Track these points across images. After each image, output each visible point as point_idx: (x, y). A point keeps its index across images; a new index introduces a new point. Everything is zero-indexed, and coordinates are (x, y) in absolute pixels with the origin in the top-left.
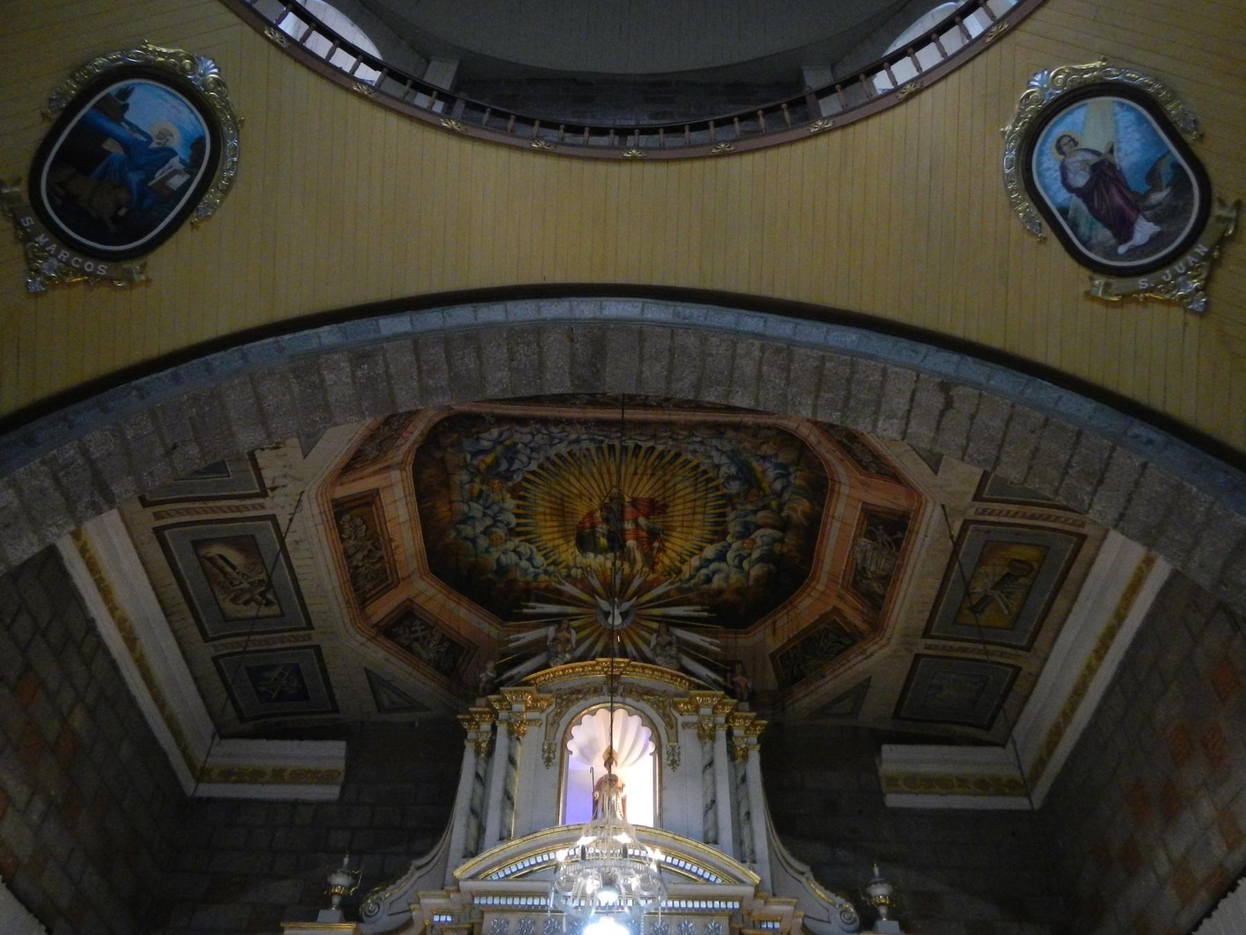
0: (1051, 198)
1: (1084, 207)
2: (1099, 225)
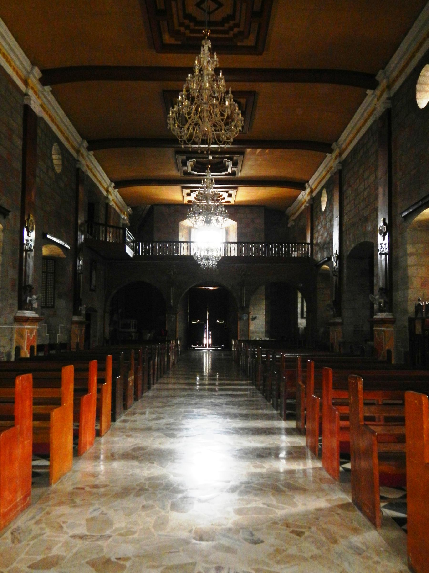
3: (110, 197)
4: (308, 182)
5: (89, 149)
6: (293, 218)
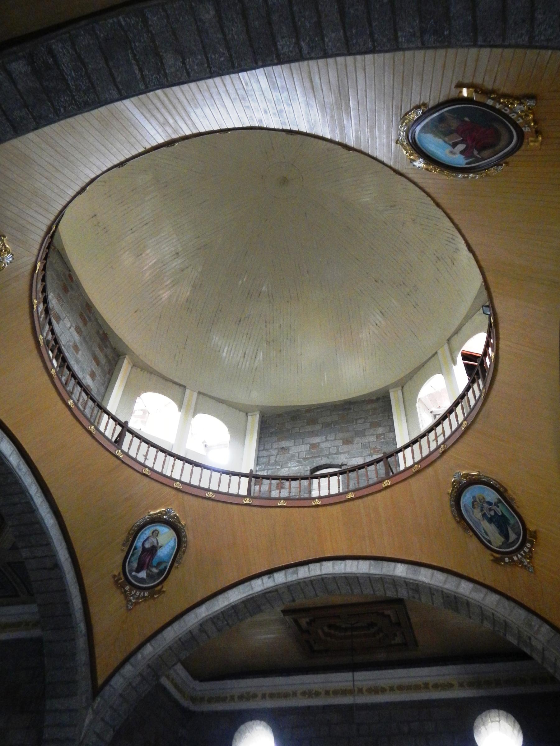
0: (137, 541)
1: (140, 553)
2: (137, 561)
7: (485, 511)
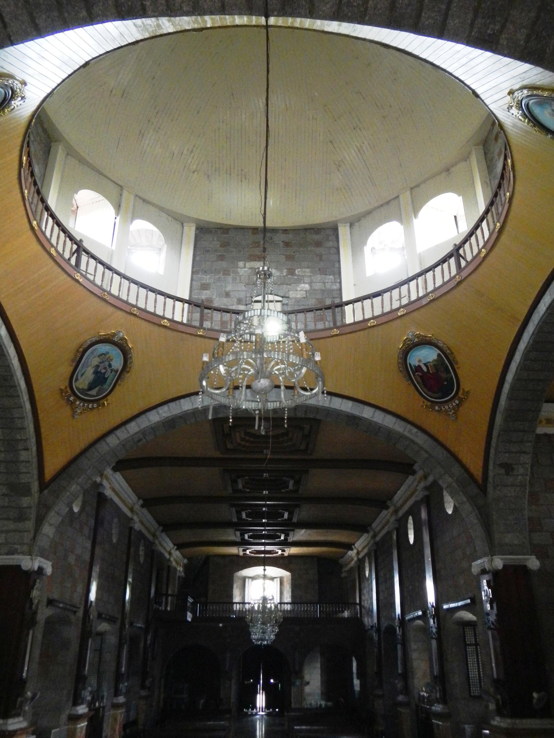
3: (172, 559)
4: (354, 544)
5: (162, 531)
6: (346, 569)
7: (101, 365)
